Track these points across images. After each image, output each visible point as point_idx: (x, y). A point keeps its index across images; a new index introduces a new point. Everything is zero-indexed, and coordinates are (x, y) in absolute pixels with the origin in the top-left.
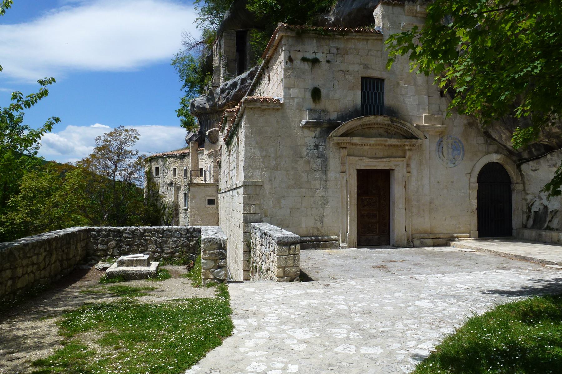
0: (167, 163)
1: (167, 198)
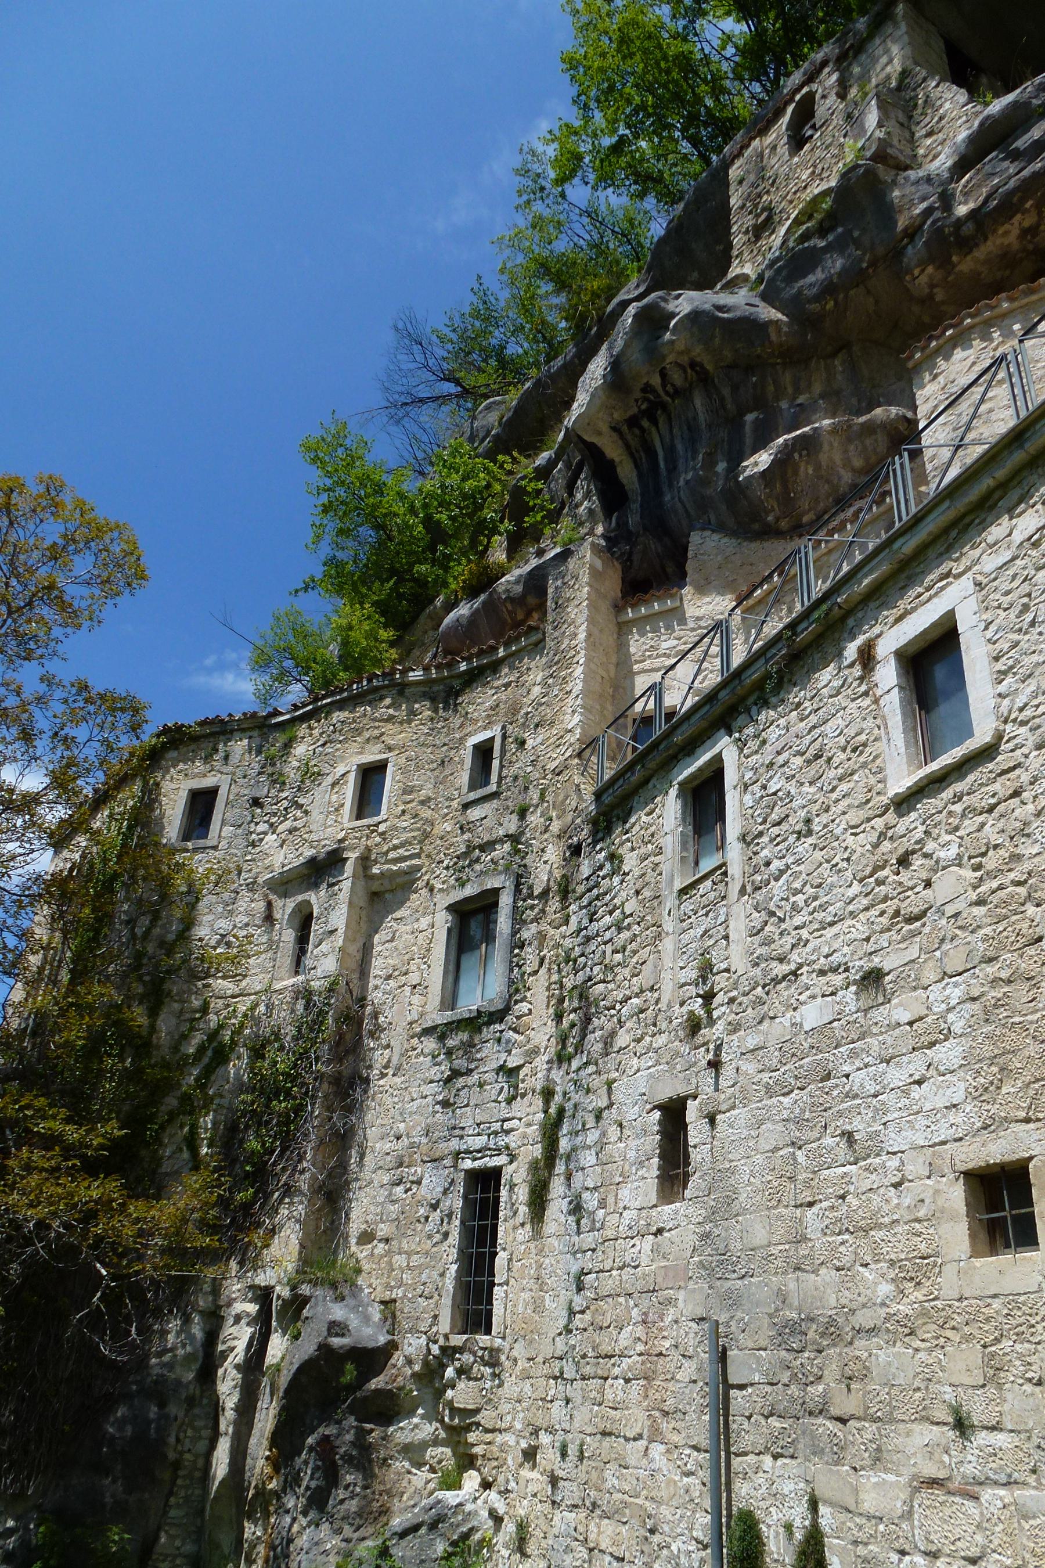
0: (300, 750)
1: (255, 982)
